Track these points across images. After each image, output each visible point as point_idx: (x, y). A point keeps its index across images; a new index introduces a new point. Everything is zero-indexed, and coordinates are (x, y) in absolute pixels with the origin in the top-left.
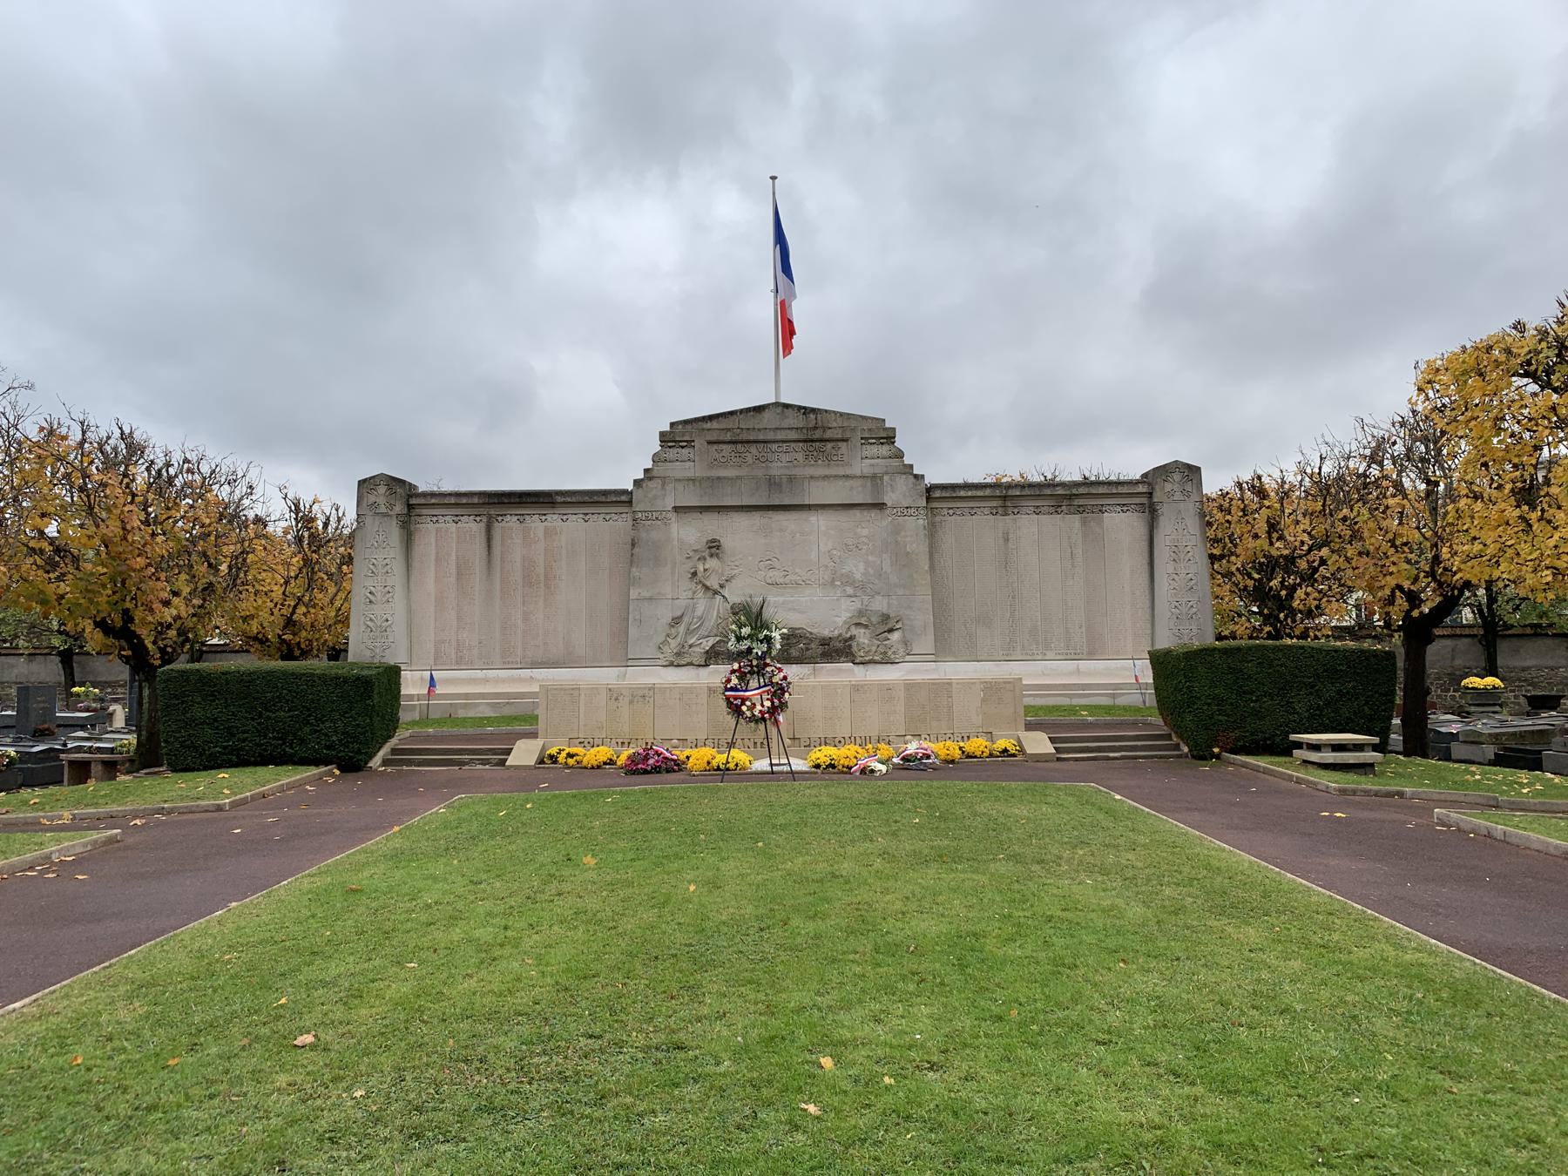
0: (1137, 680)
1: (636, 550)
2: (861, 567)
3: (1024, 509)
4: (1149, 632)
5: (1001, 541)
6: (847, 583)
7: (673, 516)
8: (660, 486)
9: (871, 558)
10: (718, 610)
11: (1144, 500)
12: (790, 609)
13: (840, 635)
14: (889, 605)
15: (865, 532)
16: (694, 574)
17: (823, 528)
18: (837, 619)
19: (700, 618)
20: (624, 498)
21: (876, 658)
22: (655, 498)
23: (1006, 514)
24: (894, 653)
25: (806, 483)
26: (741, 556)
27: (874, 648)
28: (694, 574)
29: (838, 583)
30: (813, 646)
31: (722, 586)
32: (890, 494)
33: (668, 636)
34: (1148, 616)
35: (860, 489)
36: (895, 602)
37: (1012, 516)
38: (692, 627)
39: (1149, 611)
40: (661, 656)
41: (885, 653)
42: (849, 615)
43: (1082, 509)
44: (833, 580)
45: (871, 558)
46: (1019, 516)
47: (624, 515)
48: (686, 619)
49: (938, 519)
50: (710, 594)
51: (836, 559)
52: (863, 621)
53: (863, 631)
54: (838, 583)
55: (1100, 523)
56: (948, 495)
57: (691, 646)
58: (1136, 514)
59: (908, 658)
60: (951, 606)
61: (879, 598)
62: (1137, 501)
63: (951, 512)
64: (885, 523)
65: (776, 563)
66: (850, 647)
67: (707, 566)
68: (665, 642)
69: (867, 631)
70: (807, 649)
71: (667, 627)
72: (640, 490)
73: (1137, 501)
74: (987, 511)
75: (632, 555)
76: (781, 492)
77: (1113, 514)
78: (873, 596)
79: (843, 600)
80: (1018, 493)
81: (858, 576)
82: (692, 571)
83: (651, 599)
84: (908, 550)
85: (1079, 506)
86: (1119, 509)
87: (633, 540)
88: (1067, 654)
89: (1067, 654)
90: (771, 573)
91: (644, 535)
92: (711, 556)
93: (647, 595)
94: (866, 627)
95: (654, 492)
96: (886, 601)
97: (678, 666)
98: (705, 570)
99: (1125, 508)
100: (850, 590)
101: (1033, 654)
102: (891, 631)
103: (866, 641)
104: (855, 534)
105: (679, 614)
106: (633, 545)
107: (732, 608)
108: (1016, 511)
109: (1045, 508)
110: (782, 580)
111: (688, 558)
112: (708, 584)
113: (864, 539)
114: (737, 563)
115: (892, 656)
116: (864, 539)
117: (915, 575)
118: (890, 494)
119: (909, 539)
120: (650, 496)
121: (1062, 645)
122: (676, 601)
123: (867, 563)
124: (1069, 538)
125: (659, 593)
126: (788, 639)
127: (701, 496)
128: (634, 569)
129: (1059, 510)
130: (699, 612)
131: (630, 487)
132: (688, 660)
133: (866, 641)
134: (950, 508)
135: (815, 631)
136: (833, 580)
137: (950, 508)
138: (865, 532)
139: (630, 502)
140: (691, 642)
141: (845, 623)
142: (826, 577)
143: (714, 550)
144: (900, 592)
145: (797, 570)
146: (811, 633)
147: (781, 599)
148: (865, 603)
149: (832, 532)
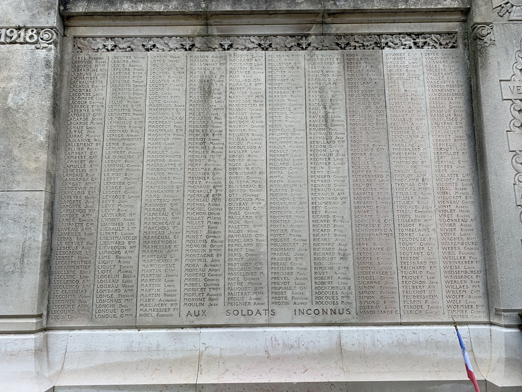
0: (470, 374)
3: (241, 40)
4: (478, 266)
5: (197, 95)
11: (454, 26)
23: (209, 49)
34: (474, 236)
37: (218, 53)
39: (474, 225)
43: (343, 41)
46: (231, 51)
49: (83, 55)
55: (379, 60)
56: (100, 9)
58: (440, 50)
60: (94, 215)
62: (442, 27)
63: (110, 44)
73: (442, 27)
74: (172, 44)
77: (400, 51)
80: (228, 8)
84: (10, 103)
85: (339, 36)
86: (409, 42)
88: (317, 312)
89: (317, 312)
99: (420, 41)
101: (250, 313)
108: (226, 43)
109: (278, 40)
117: (16, 152)
119: (14, 83)
121: (308, 294)
124: (322, 90)
129: (304, 42)
134: (107, 38)
137: (107, 38)
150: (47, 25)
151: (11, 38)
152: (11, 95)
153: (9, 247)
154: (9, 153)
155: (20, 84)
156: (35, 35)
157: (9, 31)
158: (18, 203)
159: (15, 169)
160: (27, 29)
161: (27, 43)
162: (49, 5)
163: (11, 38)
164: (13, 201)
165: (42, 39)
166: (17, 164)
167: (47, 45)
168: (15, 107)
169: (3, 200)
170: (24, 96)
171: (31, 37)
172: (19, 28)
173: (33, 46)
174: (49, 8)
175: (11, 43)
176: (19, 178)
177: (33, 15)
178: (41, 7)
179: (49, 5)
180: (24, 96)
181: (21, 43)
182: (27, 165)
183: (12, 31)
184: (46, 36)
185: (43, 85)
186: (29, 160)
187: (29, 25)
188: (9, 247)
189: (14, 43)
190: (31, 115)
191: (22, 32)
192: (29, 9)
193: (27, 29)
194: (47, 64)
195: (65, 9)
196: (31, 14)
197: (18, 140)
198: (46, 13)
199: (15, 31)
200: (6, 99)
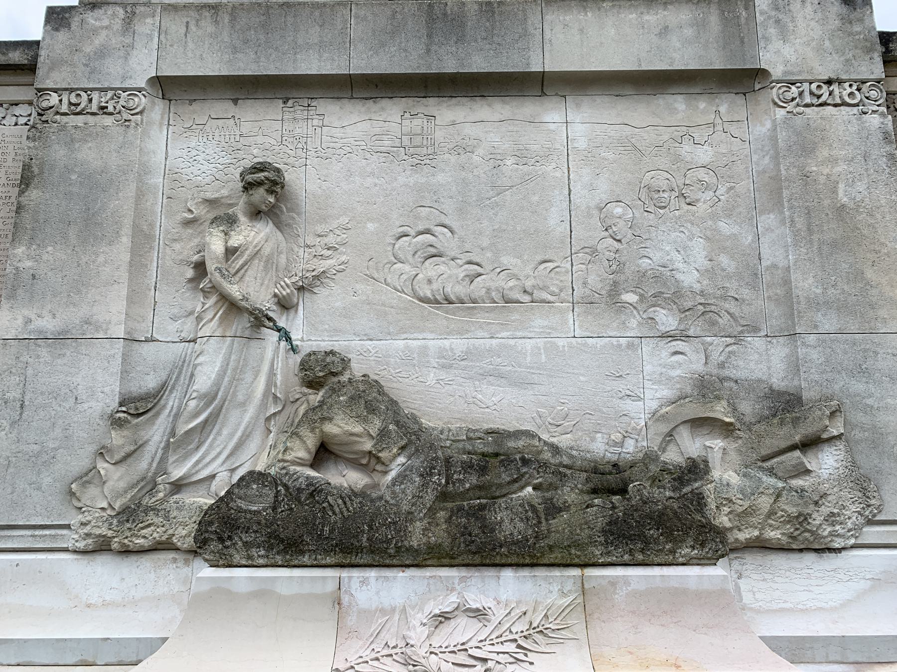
1: (34, 194)
2: (699, 250)
6: (658, 300)
7: (157, 110)
8: (118, 25)
9: (726, 227)
10: (272, 374)
12: (484, 375)
13: (649, 458)
14: (795, 366)
15: (704, 154)
16: (200, 268)
17: (582, 144)
18: (631, 406)
19: (209, 398)
20: (16, 57)
21: (773, 534)
22: (102, 53)
24: (831, 519)
25: (534, 19)
26: (344, 220)
27: (765, 503)
28: (200, 268)
29: (630, 298)
30: (569, 494)
31: (285, 305)
32: (777, 44)
33: (102, 453)
35: (689, 32)
36: (814, 355)
38: (182, 429)
40: (74, 519)
41: (802, 519)
42: (666, 393)
44: (614, 291)
45: (726, 227)
47: (18, 110)
48: (171, 402)
50: (242, 324)
51: (621, 228)
52: (720, 411)
53: (717, 443)
54: (630, 298)
57: (178, 486)
59: (872, 534)
61: (756, 342)
64: (762, 128)
65: (443, 240)
66: (699, 500)
67: (235, 240)
68: (89, 477)
69: (732, 446)
70: (553, 509)
71: (104, 424)
72: (62, 36)
75: (19, 208)
76: (461, 39)
78: (738, 339)
79: (647, 347)
81: (689, 278)
82: (196, 258)
83: (61, 338)
87: (27, 167)
90: (431, 269)
91: (58, 153)
92: (256, 214)
93: (47, 324)
94: (727, 430)
95: (98, 41)
96: (779, 353)
97: (126, 552)
98: (230, 252)
100: (667, 320)
102: (810, 444)
103: (733, 478)
104: (677, 159)
105: (151, 383)
106: (26, 180)
107: (304, 366)
110: (454, 289)
111: (188, 223)
112: (234, 291)
113: (702, 174)
114: (331, 240)
115: (827, 530)
116: (702, 174)
117: (869, 274)
118: (777, 44)
119: (841, 168)
120: (88, 49)
122: (147, 349)
123: (716, 243)
125: (87, 322)
126: (483, 470)
127: (235, 50)
128: (20, 250)
130: (204, 381)
131: (34, 30)
132: (156, 534)
133: (733, 478)
135: (563, 441)
136: (614, 291)
138: (704, 154)
139: (30, 68)
140: (177, 473)
141: (656, 417)
142: (592, 279)
143: (259, 194)
144: (828, 323)
145: (507, 260)
146: (556, 450)
147: (458, 344)
148: (716, 356)
149: (610, 155)
150: (872, 77)
151: (819, 97)
152: (841, 187)
153: (891, 418)
154: (857, 276)
155: (851, 169)
156: (856, 92)
157: (814, 86)
158: (890, 351)
159: (874, 299)
160: (840, 82)
161: (844, 104)
162: (868, 45)
163: (819, 97)
164: (882, 348)
165: (867, 98)
166: (874, 292)
167: (875, 108)
168: (852, 205)
169: (868, 346)
170: (861, 186)
171: (851, 94)
172: (829, 82)
173: (855, 110)
174: (869, 50)
175: (821, 105)
176: (883, 313)
177: (847, 61)
178: (856, 48)
179: (868, 45)
180: (861, 186)
181: (836, 105)
182: (891, 294)
183: (819, 87)
184: (873, 94)
185: (888, 170)
186: (892, 286)
187: (844, 77)
188: (891, 418)
189: (824, 104)
190: (879, 216)
191: (835, 87)
192: (839, 51)
193: (840, 82)
194: (886, 137)
195: (887, 48)
196: (842, 59)
197: (868, 255)
198: (867, 58)
199: (825, 87)
200: (834, 191)
